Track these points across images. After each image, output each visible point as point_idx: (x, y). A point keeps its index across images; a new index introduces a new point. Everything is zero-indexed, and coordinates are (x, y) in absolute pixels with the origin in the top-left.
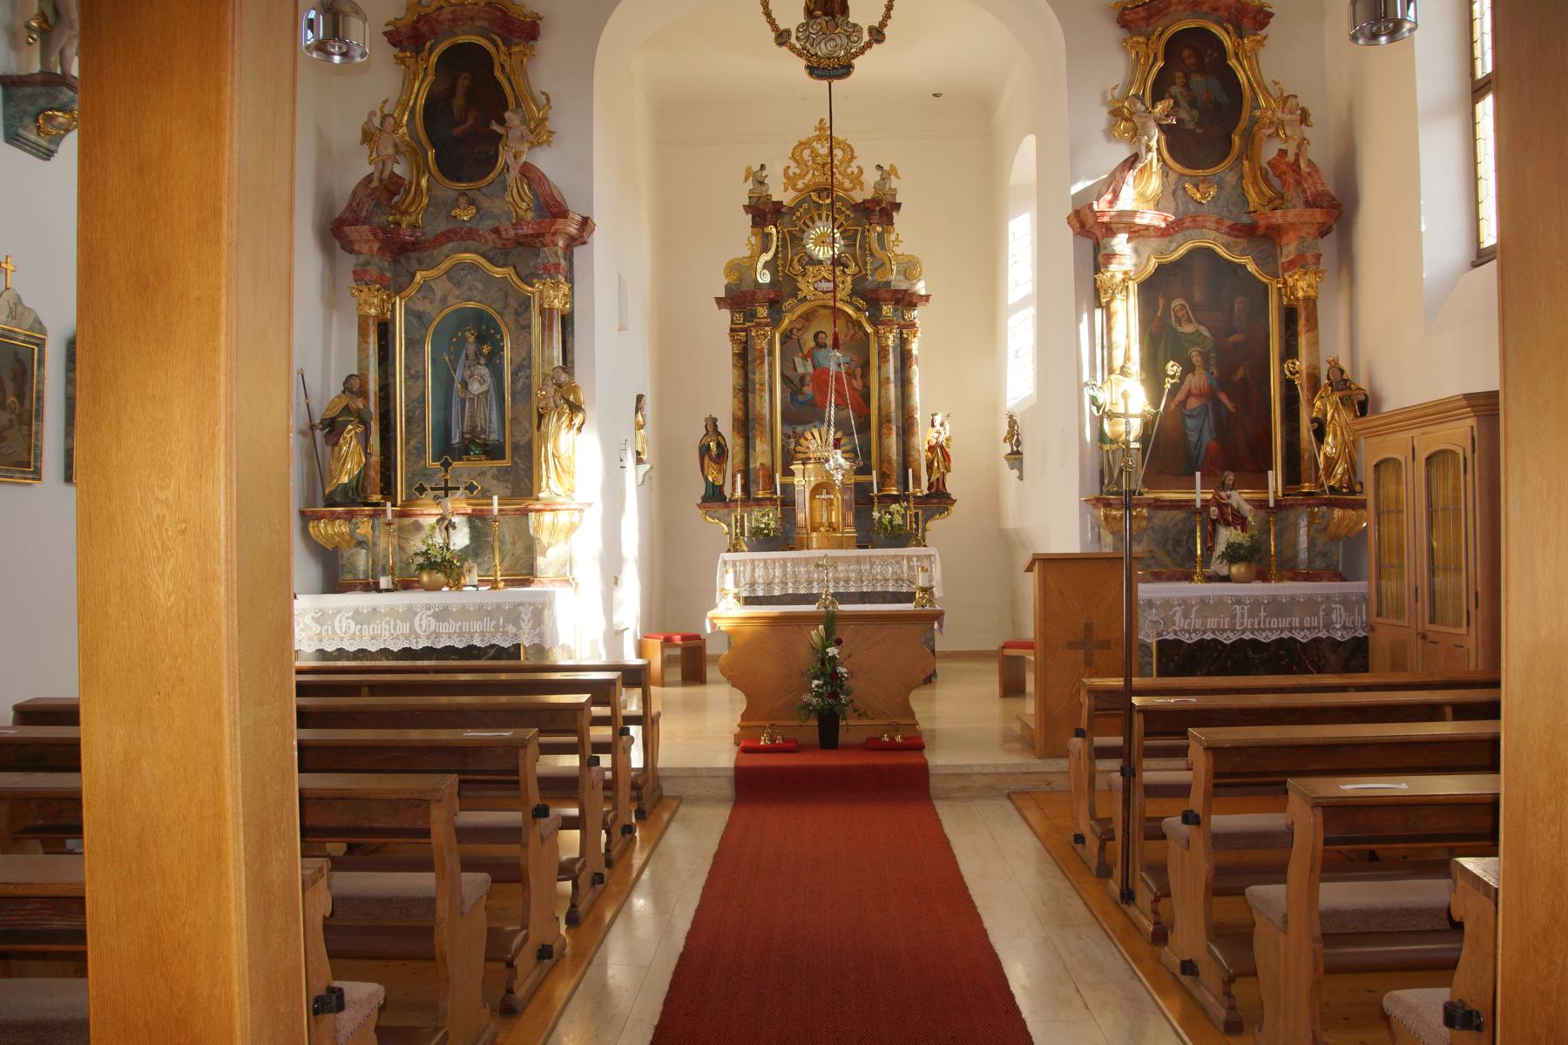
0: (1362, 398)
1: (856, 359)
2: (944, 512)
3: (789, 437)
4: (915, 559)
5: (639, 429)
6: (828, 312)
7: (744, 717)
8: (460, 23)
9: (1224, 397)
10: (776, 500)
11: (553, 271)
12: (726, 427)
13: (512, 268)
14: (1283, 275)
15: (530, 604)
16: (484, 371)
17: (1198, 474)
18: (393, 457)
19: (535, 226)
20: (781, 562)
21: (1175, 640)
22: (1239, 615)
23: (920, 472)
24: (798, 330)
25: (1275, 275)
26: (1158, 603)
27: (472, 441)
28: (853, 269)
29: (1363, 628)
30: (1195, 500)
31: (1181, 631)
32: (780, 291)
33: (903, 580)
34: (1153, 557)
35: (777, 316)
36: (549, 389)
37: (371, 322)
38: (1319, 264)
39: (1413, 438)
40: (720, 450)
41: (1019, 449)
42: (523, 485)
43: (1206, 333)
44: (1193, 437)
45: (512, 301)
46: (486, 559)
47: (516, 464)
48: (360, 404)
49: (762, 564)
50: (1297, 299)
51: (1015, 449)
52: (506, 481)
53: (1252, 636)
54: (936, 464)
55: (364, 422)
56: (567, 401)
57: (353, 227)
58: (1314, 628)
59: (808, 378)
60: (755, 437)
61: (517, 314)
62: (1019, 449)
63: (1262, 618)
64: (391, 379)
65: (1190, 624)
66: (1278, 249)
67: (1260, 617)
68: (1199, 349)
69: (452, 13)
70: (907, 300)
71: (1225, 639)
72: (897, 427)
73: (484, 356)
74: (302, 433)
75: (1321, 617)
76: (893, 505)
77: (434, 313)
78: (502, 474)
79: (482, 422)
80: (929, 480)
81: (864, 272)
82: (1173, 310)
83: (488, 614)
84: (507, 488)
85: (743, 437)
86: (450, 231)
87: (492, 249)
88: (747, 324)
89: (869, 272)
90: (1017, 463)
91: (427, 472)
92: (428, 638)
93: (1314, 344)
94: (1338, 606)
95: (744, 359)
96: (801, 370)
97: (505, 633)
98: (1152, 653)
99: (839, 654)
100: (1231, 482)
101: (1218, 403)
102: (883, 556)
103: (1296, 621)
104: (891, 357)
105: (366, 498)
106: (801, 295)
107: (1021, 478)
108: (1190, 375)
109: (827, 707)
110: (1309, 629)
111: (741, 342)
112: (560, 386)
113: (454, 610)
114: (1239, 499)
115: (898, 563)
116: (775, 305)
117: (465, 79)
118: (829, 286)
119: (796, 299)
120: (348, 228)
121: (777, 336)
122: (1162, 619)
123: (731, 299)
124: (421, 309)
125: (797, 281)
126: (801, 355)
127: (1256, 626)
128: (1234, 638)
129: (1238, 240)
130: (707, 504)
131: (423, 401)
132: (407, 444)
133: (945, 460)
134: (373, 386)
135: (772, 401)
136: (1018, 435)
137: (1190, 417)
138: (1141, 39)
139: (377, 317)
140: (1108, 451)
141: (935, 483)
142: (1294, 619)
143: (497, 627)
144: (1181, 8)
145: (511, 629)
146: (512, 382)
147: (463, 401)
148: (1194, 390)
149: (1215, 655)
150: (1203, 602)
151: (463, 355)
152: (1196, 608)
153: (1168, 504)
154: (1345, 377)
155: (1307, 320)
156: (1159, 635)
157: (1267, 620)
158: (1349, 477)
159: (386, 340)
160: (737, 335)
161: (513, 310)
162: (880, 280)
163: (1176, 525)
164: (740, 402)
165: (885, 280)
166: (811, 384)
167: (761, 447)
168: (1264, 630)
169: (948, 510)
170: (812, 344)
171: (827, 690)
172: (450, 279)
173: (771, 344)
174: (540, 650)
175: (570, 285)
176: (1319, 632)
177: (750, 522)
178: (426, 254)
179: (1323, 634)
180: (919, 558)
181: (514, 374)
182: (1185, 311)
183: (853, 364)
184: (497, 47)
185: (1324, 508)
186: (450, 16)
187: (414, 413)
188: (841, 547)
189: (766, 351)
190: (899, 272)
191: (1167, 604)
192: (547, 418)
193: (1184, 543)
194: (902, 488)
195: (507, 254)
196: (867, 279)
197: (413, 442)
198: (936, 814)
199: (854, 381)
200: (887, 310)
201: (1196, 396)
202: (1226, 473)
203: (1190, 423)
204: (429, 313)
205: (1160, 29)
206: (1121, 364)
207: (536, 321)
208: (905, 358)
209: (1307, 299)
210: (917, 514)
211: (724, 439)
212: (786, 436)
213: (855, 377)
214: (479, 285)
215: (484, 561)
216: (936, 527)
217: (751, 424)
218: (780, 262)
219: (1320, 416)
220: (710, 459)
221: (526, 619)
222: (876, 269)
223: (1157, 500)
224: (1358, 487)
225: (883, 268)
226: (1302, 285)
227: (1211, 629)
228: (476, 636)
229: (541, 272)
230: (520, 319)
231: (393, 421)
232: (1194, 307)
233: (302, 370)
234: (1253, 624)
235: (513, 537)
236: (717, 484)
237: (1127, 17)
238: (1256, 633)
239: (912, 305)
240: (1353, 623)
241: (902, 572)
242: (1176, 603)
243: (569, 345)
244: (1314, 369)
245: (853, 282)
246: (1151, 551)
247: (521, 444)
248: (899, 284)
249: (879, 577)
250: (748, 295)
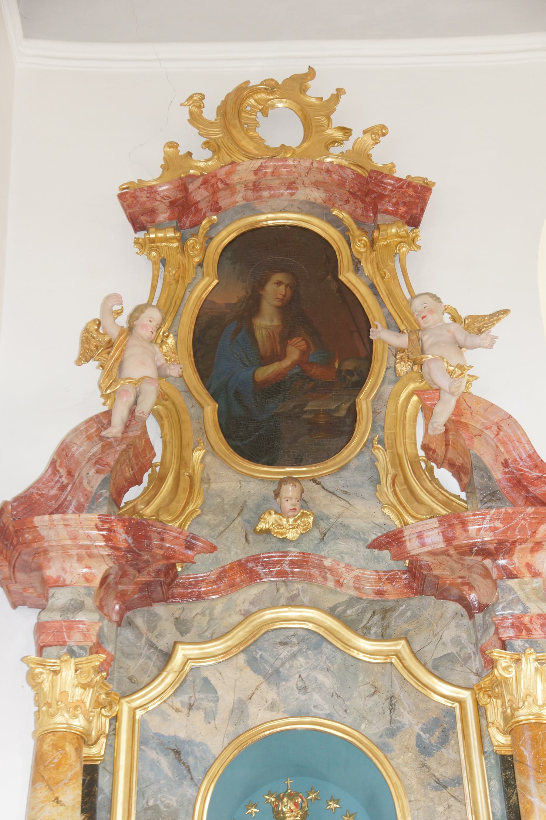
8: (266, 194)
13: (403, 642)
19: (498, 524)
57: (56, 517)
69: (256, 172)
86: (256, 559)
87: (352, 602)
117: (279, 283)
120: (46, 517)
124: (182, 735)
161: (413, 742)
178: (197, 607)
184: (345, 232)
186: (253, 178)
195: (386, 612)
204: (201, 744)
229: (511, 633)
230: (432, 763)
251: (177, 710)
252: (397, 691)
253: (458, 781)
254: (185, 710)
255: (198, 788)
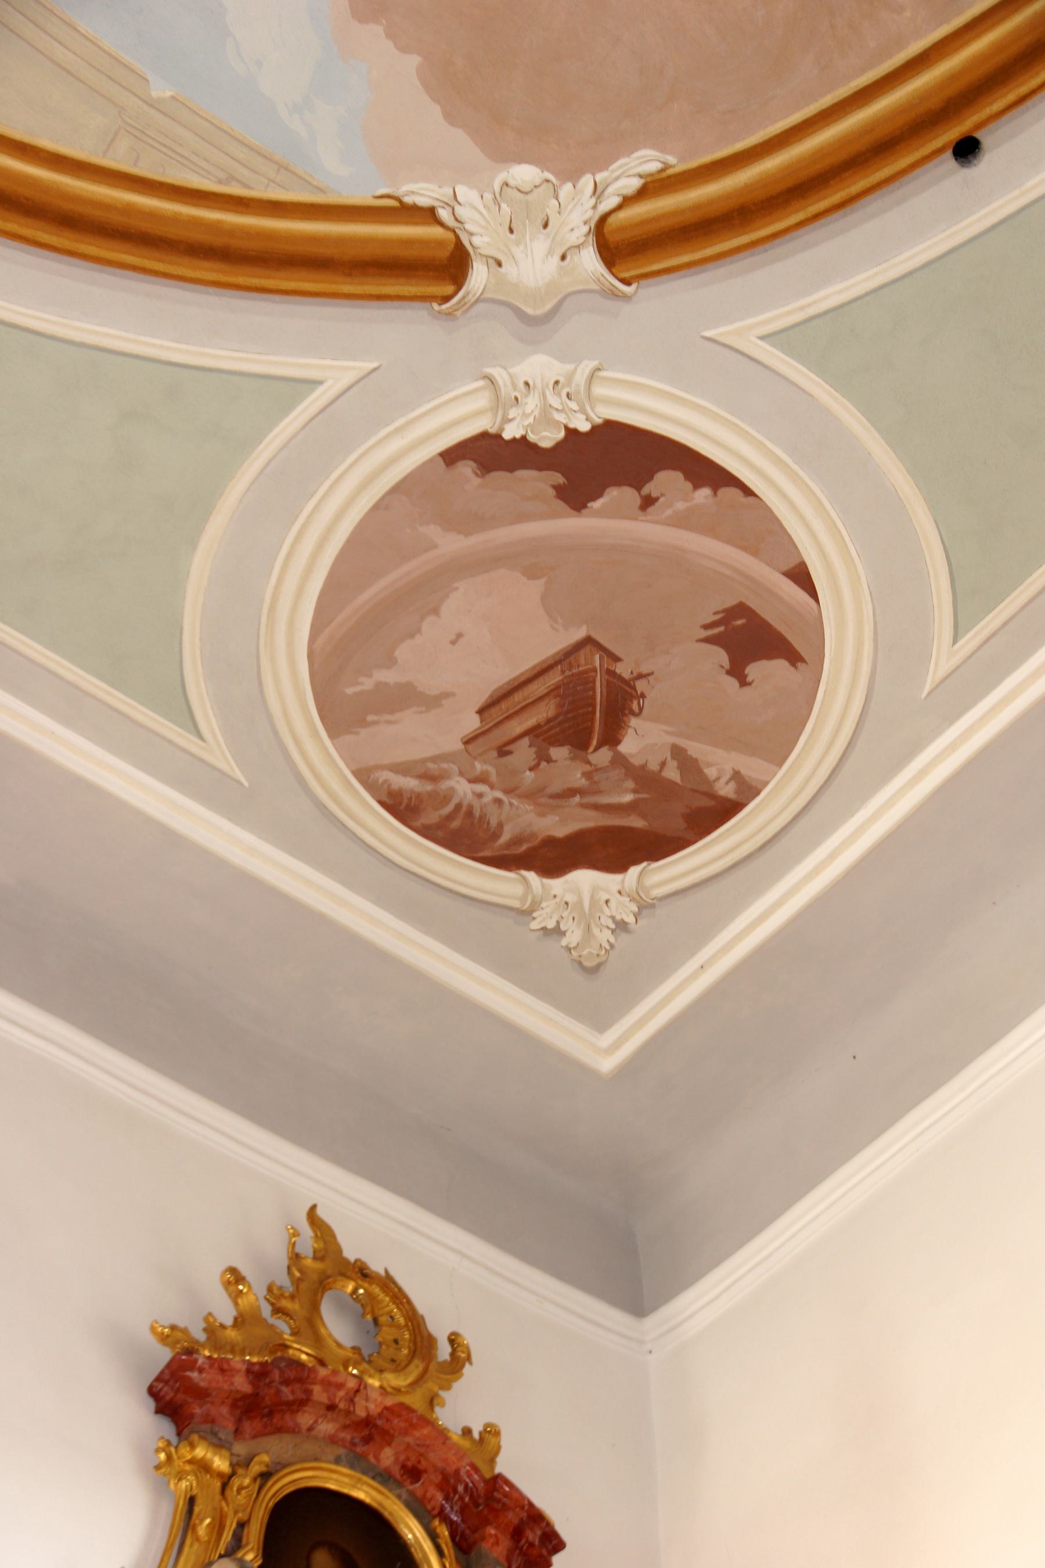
138: (220, 1463)
144: (327, 1427)
205: (265, 1458)
237: (194, 1375)
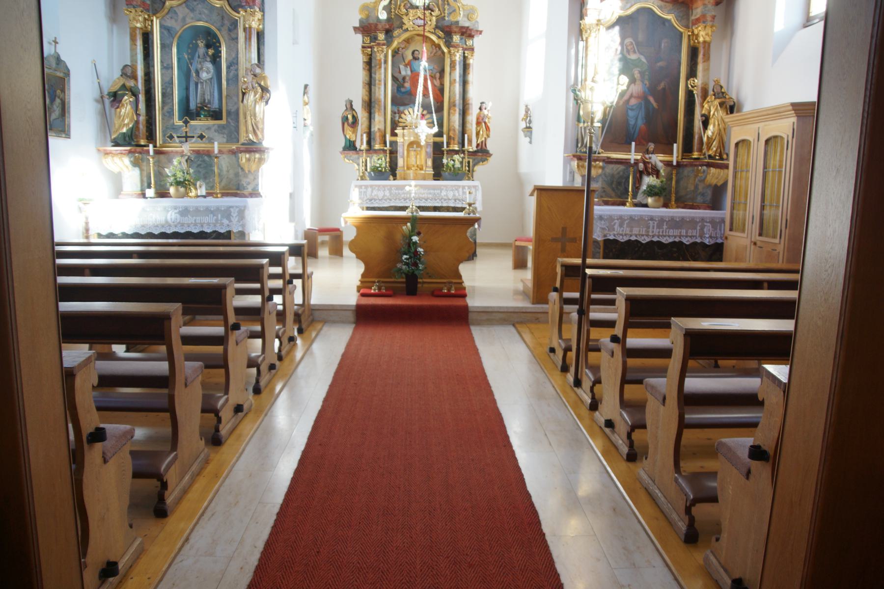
0: (732, 103)
1: (436, 68)
2: (485, 161)
3: (395, 113)
4: (466, 188)
5: (305, 105)
6: (421, 38)
7: (363, 276)
9: (651, 99)
10: (386, 151)
11: (251, 4)
12: (358, 107)
14: (692, 27)
15: (237, 207)
16: (209, 65)
17: (633, 144)
18: (154, 117)
20: (389, 187)
21: (614, 240)
22: (651, 227)
23: (472, 137)
24: (403, 48)
25: (687, 27)
26: (606, 217)
27: (202, 108)
28: (436, 12)
29: (721, 238)
30: (630, 159)
31: (617, 234)
32: (392, 24)
33: (459, 200)
34: (604, 191)
35: (390, 40)
36: (249, 77)
37: (138, 32)
38: (714, 21)
39: (759, 128)
40: (354, 121)
41: (531, 125)
42: (233, 136)
43: (644, 60)
44: (632, 122)
45: (226, 22)
46: (211, 180)
47: (229, 123)
48: (131, 83)
49: (377, 188)
50: (699, 42)
51: (528, 125)
52: (223, 133)
53: (658, 239)
54: (481, 132)
55: (135, 94)
56: (260, 85)
58: (694, 236)
59: (407, 78)
60: (375, 113)
61: (230, 30)
62: (531, 125)
63: (665, 229)
64: (151, 69)
65: (623, 231)
66: (691, 11)
67: (663, 228)
68: (639, 69)
70: (467, 33)
71: (643, 240)
72: (460, 110)
73: (209, 56)
74: (97, 101)
75: (698, 231)
76: (455, 156)
77: (178, 28)
78: (221, 128)
79: (209, 97)
80: (477, 142)
81: (443, 15)
82: (626, 45)
83: (212, 212)
84: (224, 137)
85: (368, 112)
88: (372, 44)
89: (446, 15)
90: (529, 133)
91: (174, 127)
92: (176, 226)
93: (707, 70)
94: (708, 224)
95: (370, 64)
96: (403, 73)
97: (222, 224)
98: (600, 246)
99: (419, 240)
100: (652, 149)
101: (647, 102)
102: (449, 185)
103: (684, 232)
104: (457, 67)
105: (137, 142)
106: (405, 27)
107: (530, 142)
108: (633, 84)
109: (411, 271)
110: (691, 237)
111: (368, 55)
112: (255, 75)
113: (191, 210)
114: (657, 159)
115: (456, 190)
116: (388, 32)
118: (421, 22)
119: (402, 29)
121: (390, 52)
122: (607, 227)
123: (363, 28)
124: (169, 25)
125: (403, 19)
126: (404, 64)
127: (661, 234)
128: (648, 240)
129: (667, 4)
130: (345, 152)
131: (171, 83)
132: (163, 108)
133: (487, 130)
134: (140, 73)
135: (385, 91)
136: (530, 117)
137: (632, 110)
139: (141, 29)
140: (581, 128)
141: (480, 144)
142: (682, 231)
143: (217, 220)
145: (226, 222)
146: (227, 73)
147: (197, 84)
148: (634, 94)
149: (637, 249)
150: (631, 218)
151: (197, 55)
152: (627, 222)
153: (615, 160)
154: (723, 90)
155: (704, 55)
156: (605, 236)
157: (667, 230)
158: (721, 151)
159: (148, 45)
160: (366, 50)
162: (453, 20)
163: (619, 173)
164: (367, 91)
165: (455, 20)
166: (409, 82)
167: (378, 118)
168: (665, 236)
169: (487, 160)
170: (410, 57)
171: (411, 261)
172: (187, 7)
173: (386, 56)
174: (242, 234)
175: (262, 13)
176: (696, 238)
177: (371, 163)
179: (699, 240)
180: (469, 187)
181: (228, 67)
182: (632, 46)
183: (435, 71)
185: (705, 168)
187: (166, 90)
188: (424, 179)
189: (383, 61)
190: (464, 15)
191: (611, 218)
192: (247, 95)
193: (623, 184)
194: (461, 146)
196: (445, 19)
197: (166, 108)
198: (472, 334)
199: (434, 81)
200: (456, 38)
201: (635, 97)
202: (650, 144)
203: (631, 113)
206: (593, 76)
207: (241, 35)
208: (465, 67)
209: (705, 42)
210: (469, 162)
211: (356, 113)
212: (393, 113)
213: (435, 78)
214: (206, 11)
215: (210, 181)
216: (479, 169)
217: (373, 105)
218: (393, 6)
219: (706, 113)
220: (348, 124)
221: (235, 215)
222: (450, 13)
223: (609, 158)
224: (725, 156)
225: (455, 13)
226: (703, 34)
227: (635, 234)
228: (205, 225)
231: (153, 95)
232: (637, 44)
233: (94, 60)
234: (659, 232)
235: (228, 167)
236: (351, 140)
238: (660, 237)
239: (471, 36)
240: (716, 234)
241: (459, 195)
242: (616, 218)
243: (261, 51)
244: (705, 85)
245: (437, 21)
246: (603, 188)
247: (232, 111)
248: (464, 22)
249: (445, 198)
250: (373, 26)
251: (168, 19)
252: (224, 14)
253: (237, 38)
254: (170, 18)
255: (173, 38)
